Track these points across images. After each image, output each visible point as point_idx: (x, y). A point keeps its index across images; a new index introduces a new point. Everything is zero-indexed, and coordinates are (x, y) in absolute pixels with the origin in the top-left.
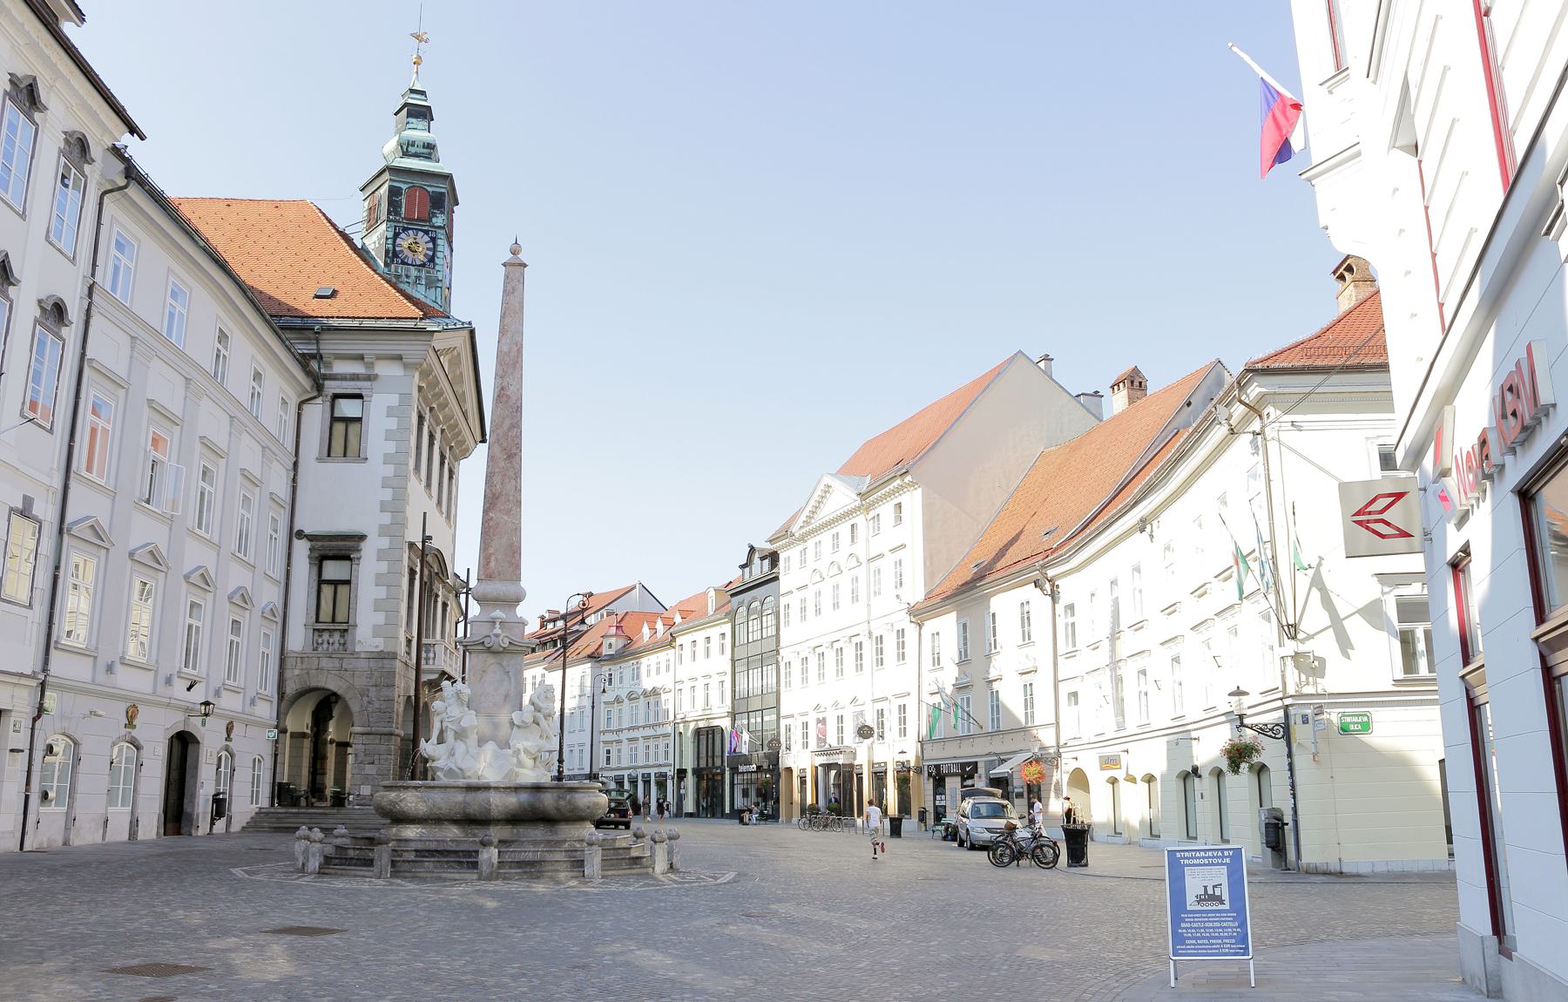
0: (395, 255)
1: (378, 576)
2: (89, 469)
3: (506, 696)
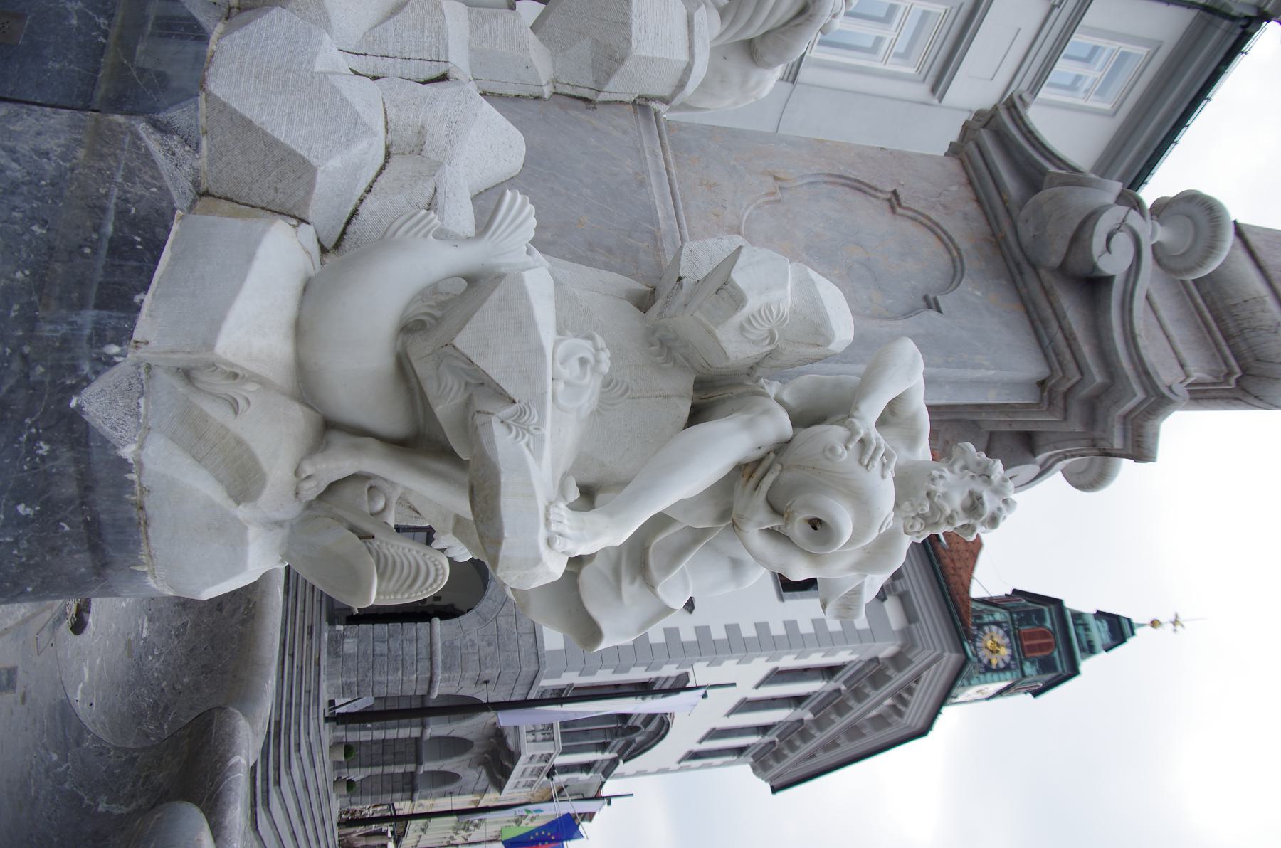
0: (980, 627)
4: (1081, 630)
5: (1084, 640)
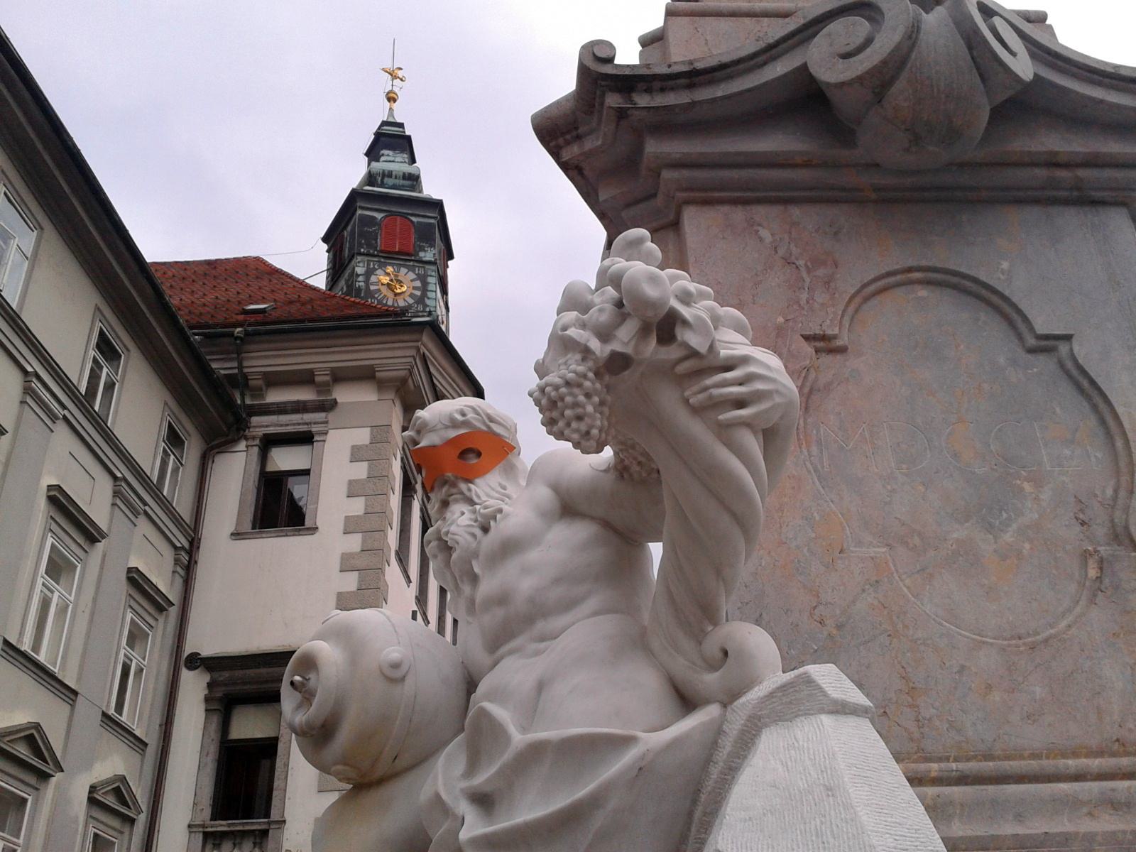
4: (388, 181)
5: (402, 182)
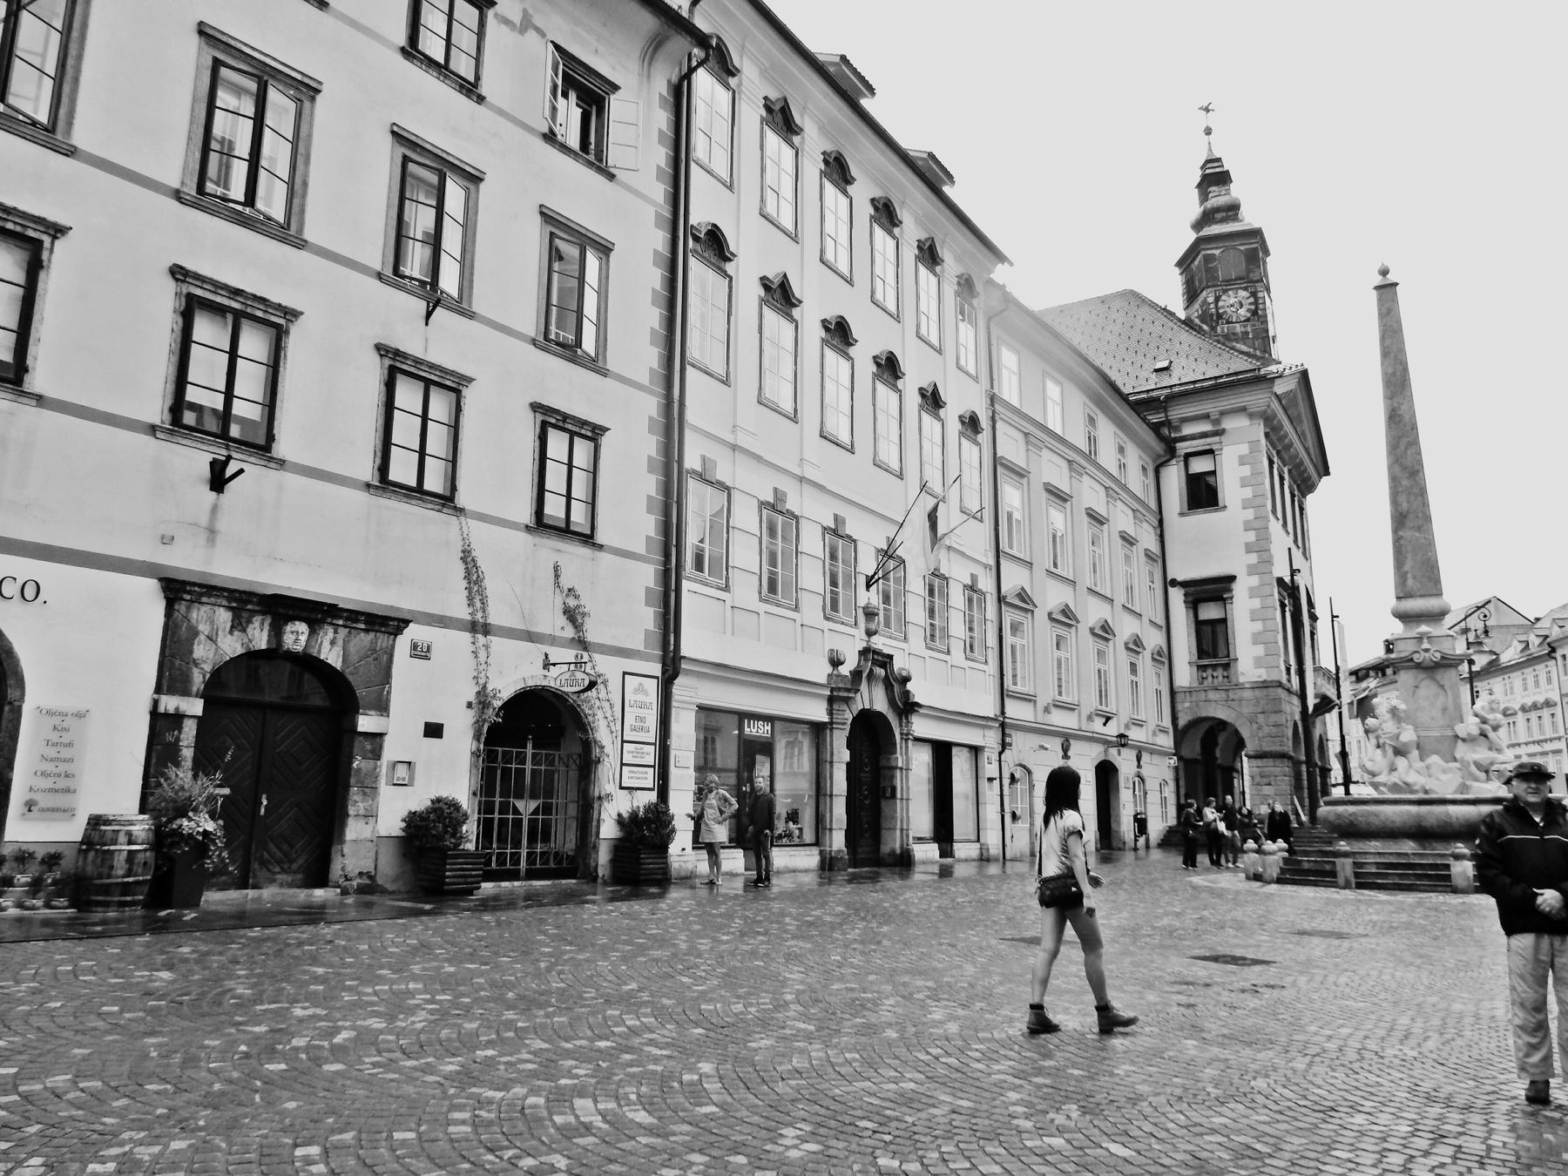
0: (1220, 316)
1: (1253, 612)
2: (1011, 547)
3: (1445, 709)
4: (1219, 216)
